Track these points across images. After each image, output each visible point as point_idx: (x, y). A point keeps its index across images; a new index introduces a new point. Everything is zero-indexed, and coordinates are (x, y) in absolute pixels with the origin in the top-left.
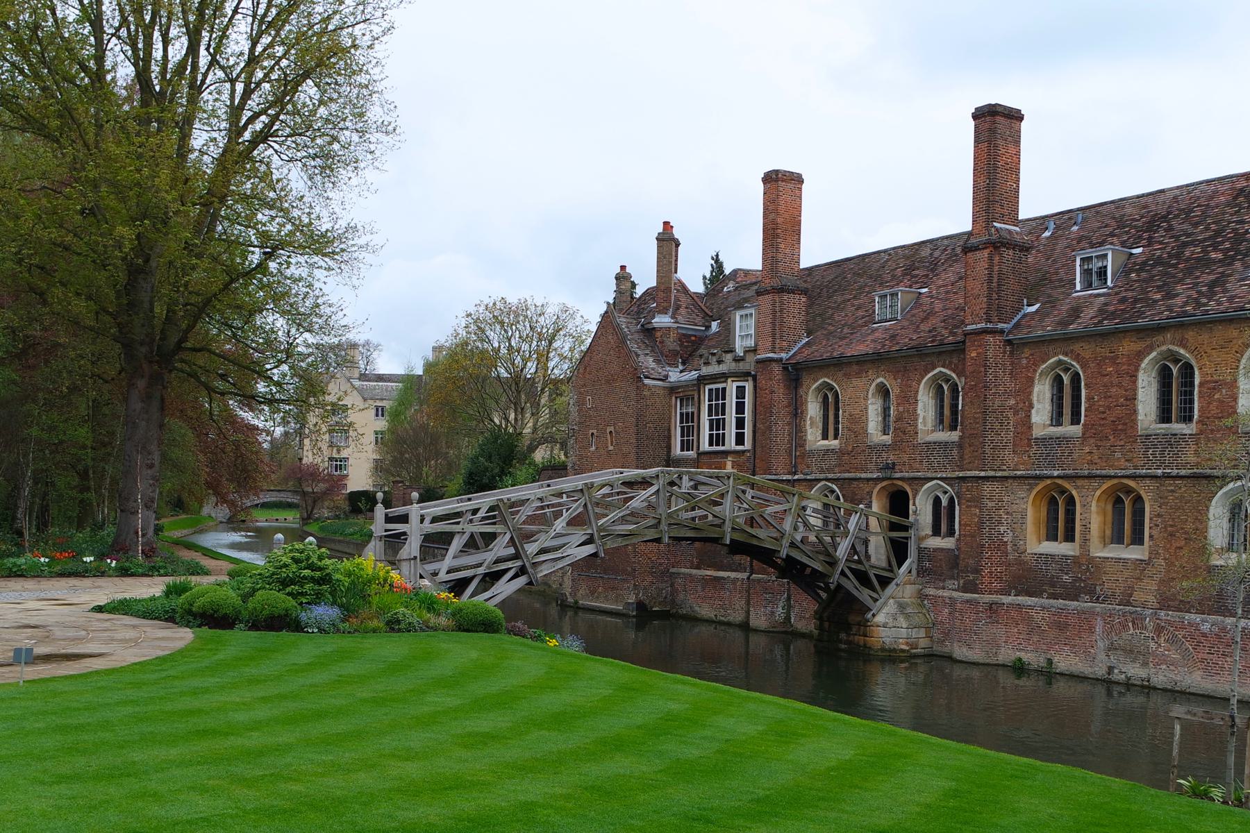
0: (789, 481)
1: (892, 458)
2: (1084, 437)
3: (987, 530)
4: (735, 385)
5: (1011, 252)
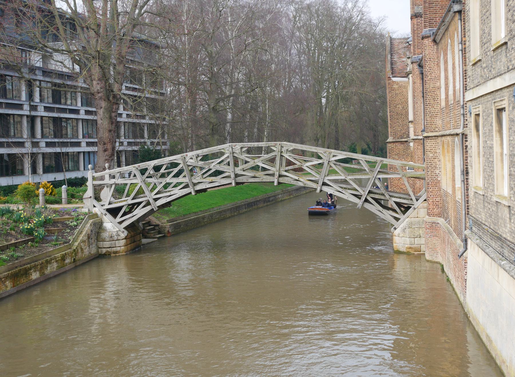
3: (430, 173)
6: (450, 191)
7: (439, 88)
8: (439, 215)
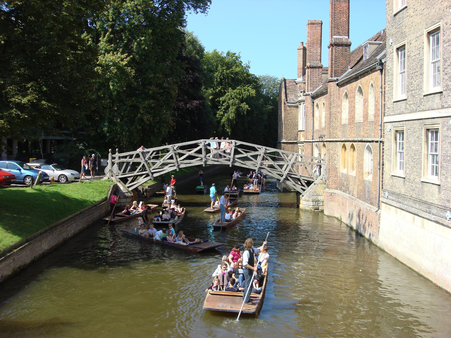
0: (311, 142)
1: (325, 133)
2: (348, 124)
4: (304, 104)
5: (341, 48)
6: (353, 173)
7: (340, 112)
8: (336, 188)
